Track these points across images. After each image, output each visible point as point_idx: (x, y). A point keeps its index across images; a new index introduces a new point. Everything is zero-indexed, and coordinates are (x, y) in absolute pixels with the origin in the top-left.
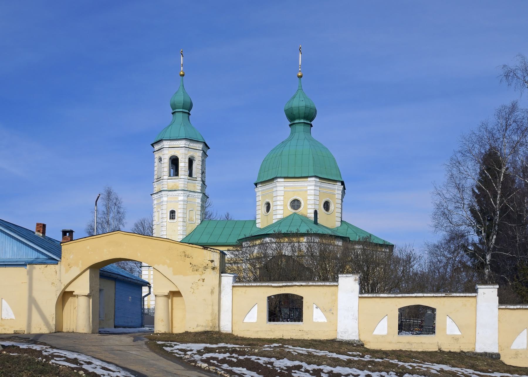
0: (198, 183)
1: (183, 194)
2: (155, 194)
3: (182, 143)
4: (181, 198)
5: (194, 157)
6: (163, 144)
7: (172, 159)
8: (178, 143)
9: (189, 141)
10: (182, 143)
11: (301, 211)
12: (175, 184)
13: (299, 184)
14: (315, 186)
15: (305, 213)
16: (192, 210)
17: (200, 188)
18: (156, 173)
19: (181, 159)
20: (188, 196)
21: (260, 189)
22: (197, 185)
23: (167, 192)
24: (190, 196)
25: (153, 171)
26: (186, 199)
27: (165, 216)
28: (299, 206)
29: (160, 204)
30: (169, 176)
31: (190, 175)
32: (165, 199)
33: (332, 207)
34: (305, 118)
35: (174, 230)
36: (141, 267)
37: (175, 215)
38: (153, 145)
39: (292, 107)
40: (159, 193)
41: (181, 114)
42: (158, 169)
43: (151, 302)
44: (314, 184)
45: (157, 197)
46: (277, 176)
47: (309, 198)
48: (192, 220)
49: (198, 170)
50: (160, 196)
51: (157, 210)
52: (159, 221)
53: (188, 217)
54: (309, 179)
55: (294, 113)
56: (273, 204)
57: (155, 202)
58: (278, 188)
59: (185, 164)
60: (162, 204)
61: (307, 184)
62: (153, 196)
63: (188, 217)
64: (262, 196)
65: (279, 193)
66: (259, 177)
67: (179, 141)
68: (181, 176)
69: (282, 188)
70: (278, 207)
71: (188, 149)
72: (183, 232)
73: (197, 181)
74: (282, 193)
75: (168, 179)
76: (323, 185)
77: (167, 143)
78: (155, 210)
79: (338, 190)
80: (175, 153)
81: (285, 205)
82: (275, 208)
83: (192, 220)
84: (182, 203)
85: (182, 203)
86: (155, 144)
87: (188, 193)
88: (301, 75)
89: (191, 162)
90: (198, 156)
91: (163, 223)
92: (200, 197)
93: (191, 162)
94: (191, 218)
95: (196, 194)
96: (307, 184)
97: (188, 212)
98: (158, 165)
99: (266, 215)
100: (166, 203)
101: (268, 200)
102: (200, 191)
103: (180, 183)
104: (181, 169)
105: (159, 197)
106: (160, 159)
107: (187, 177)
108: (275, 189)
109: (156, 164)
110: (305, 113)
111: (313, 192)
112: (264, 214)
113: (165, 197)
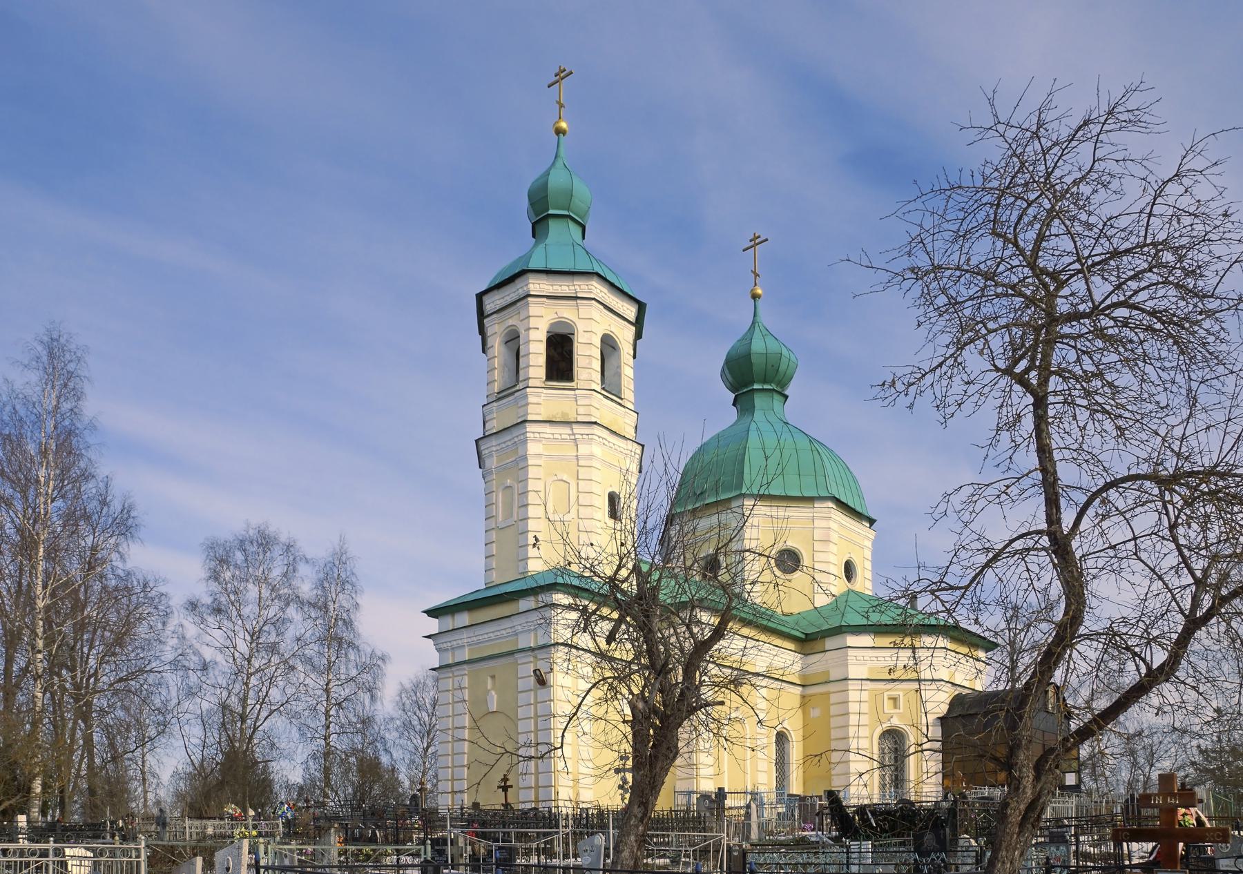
3: (630, 311)
23: (605, 434)
67: (625, 304)
96: (864, 533)
103: (627, 421)
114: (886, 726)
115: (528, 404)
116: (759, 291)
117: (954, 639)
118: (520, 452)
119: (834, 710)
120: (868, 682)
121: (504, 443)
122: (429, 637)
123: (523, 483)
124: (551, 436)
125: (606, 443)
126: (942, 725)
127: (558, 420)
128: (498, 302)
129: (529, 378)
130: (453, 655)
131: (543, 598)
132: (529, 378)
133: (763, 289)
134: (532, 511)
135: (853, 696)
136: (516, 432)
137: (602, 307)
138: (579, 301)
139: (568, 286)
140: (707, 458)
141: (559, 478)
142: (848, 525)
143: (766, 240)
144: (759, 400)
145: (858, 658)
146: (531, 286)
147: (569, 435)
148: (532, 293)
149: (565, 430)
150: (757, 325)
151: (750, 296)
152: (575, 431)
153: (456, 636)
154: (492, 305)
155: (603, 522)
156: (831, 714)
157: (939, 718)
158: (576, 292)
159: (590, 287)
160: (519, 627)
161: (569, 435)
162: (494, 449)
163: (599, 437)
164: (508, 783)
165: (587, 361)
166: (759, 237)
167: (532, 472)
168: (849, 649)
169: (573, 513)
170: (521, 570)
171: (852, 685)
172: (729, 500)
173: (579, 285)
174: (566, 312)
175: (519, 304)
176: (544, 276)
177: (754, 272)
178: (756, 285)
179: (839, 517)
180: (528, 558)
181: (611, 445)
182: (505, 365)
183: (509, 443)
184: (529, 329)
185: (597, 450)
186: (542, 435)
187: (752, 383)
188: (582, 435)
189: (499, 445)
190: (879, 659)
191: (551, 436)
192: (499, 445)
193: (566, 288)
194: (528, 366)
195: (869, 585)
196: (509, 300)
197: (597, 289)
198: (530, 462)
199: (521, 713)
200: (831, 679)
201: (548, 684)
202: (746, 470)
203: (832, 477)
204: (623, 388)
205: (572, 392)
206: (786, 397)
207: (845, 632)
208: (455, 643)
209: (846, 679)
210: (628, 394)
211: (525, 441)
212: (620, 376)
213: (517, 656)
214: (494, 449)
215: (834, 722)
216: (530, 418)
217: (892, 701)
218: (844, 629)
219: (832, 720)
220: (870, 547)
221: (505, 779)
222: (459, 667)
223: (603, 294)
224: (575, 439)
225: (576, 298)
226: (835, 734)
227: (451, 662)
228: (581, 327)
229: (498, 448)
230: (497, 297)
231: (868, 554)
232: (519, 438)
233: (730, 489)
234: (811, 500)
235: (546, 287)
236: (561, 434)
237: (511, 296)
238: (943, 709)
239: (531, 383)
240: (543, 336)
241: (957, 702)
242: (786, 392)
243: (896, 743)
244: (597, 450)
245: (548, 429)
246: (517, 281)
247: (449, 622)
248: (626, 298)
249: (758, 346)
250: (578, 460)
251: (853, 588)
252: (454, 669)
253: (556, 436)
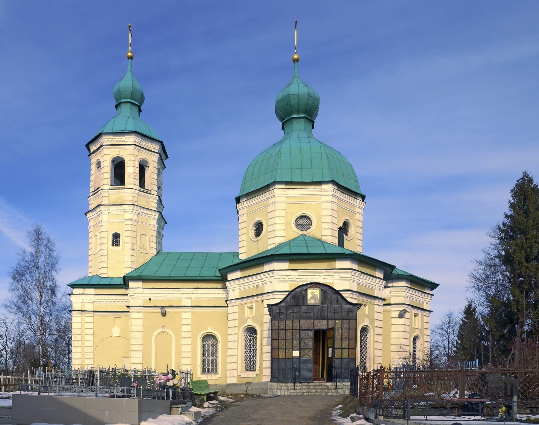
0: (153, 198)
1: (131, 210)
2: (91, 213)
3: (131, 139)
4: (129, 216)
5: (147, 162)
6: (102, 141)
7: (116, 163)
8: (123, 139)
9: (141, 136)
10: (131, 139)
11: (312, 231)
12: (119, 197)
13: (308, 193)
14: (334, 196)
15: (318, 236)
16: (145, 234)
17: (155, 205)
18: (92, 184)
19: (129, 162)
20: (139, 214)
21: (244, 205)
22: (151, 200)
23: (108, 208)
24: (142, 214)
25: (89, 181)
26: (135, 217)
27: (105, 242)
28: (309, 226)
29: (98, 225)
30: (111, 186)
31: (142, 183)
32: (105, 217)
33: (352, 231)
34: (305, 112)
35: (119, 261)
36: (70, 311)
37: (120, 241)
38: (88, 146)
39: (289, 95)
40: (96, 209)
41: (129, 105)
42: (95, 178)
43: (86, 360)
44: (332, 193)
45: (93, 217)
46: (276, 181)
47: (324, 213)
48: (144, 249)
49: (153, 179)
50: (98, 213)
51: (94, 234)
52: (96, 249)
53: (138, 243)
54: (324, 186)
55: (292, 104)
56: (267, 223)
57: (91, 224)
58: (277, 199)
59: (134, 169)
60: (100, 225)
61: (320, 193)
62: (89, 215)
63: (138, 243)
64: (249, 214)
65: (278, 206)
66: (243, 188)
67: (126, 137)
69: (283, 199)
70: (277, 227)
71: (139, 148)
72: (131, 263)
73: (151, 194)
74: (283, 206)
75: (109, 189)
76: (342, 198)
77: (108, 139)
78: (91, 235)
79: (359, 207)
80: (120, 154)
81: (287, 224)
82: (271, 228)
83: (144, 249)
84: (131, 223)
85: (131, 223)
86: (92, 144)
87: (138, 209)
88: (298, 57)
89: (142, 168)
90: (153, 160)
91: (102, 251)
92: (155, 217)
93: (142, 168)
94: (144, 245)
95: (150, 212)
96: (320, 193)
97: (138, 237)
98: (95, 173)
99: (256, 240)
100: (106, 223)
101: (258, 219)
102: (156, 210)
103: (127, 195)
104: (129, 175)
105: (97, 215)
106: (99, 164)
107: (137, 187)
108: (271, 201)
109: (92, 172)
110: (307, 104)
111: (329, 205)
112: (253, 239)
113: (105, 215)
120: (237, 301)
137: (110, 146)
163: (105, 210)
223: (111, 139)
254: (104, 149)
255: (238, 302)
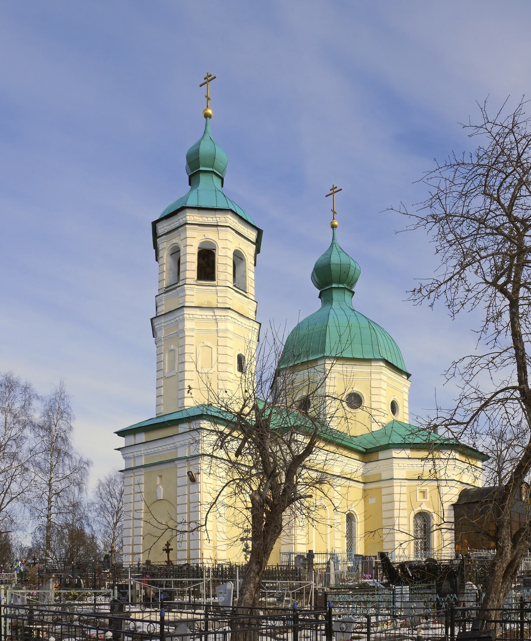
3: (252, 235)
23: (236, 316)
67: (249, 230)
68: (251, 295)
96: (403, 383)
103: (250, 307)
114: (417, 509)
115: (185, 295)
116: (336, 223)
117: (462, 453)
118: (180, 327)
119: (384, 499)
120: (406, 481)
121: (170, 321)
122: (118, 449)
123: (182, 347)
124: (200, 317)
125: (236, 322)
126: (454, 509)
127: (205, 306)
128: (166, 228)
129: (186, 278)
130: (134, 461)
131: (193, 425)
132: (186, 278)
133: (338, 223)
134: (188, 366)
135: (396, 490)
136: (177, 314)
137: (234, 232)
138: (219, 228)
139: (212, 218)
140: (302, 332)
141: (205, 345)
142: (393, 377)
143: (341, 190)
144: (336, 295)
145: (400, 465)
146: (188, 217)
147: (212, 316)
148: (188, 222)
149: (210, 313)
150: (334, 245)
151: (330, 226)
152: (216, 314)
153: (136, 449)
154: (162, 229)
155: (234, 374)
156: (383, 502)
157: (452, 505)
158: (217, 222)
159: (226, 219)
160: (178, 443)
161: (212, 316)
162: (163, 325)
163: (232, 318)
164: (170, 547)
165: (224, 268)
166: (336, 188)
167: (188, 340)
168: (394, 459)
169: (214, 368)
170: (180, 405)
171: (396, 483)
172: (316, 360)
173: (219, 218)
174: (211, 235)
175: (180, 229)
176: (196, 211)
177: (333, 211)
178: (334, 219)
179: (387, 372)
180: (185, 397)
181: (240, 323)
182: (171, 269)
183: (173, 321)
184: (187, 245)
185: (230, 326)
186: (194, 316)
187: (332, 283)
188: (220, 316)
189: (166, 322)
190: (413, 466)
191: (200, 317)
192: (166, 322)
193: (209, 219)
194: (186, 270)
195: (407, 417)
196: (173, 226)
197: (231, 220)
198: (186, 334)
199: (179, 500)
200: (383, 479)
201: (197, 481)
202: (327, 340)
203: (382, 345)
204: (247, 285)
205: (214, 288)
206: (353, 293)
207: (391, 448)
208: (135, 454)
209: (392, 479)
210: (251, 290)
211: (183, 320)
212: (246, 277)
213: (176, 462)
214: (163, 325)
215: (384, 507)
216: (186, 304)
217: (422, 494)
218: (390, 446)
219: (383, 505)
220: (407, 392)
221: (168, 544)
222: (138, 470)
223: (235, 224)
224: (216, 319)
225: (217, 226)
226: (385, 515)
227: (133, 466)
228: (220, 245)
229: (165, 324)
230: (166, 224)
231: (406, 397)
232: (179, 318)
233: (317, 353)
234: (369, 360)
235: (198, 218)
236: (207, 316)
237: (175, 224)
238: (455, 500)
239: (187, 281)
240: (196, 251)
241: (464, 494)
242: (353, 290)
243: (425, 521)
244: (230, 326)
245: (198, 312)
246: (179, 214)
247: (131, 440)
248: (250, 227)
249: (335, 259)
250: (218, 332)
251: (397, 419)
252: (134, 471)
253: (203, 317)
254: (228, 232)
255: (408, 483)
